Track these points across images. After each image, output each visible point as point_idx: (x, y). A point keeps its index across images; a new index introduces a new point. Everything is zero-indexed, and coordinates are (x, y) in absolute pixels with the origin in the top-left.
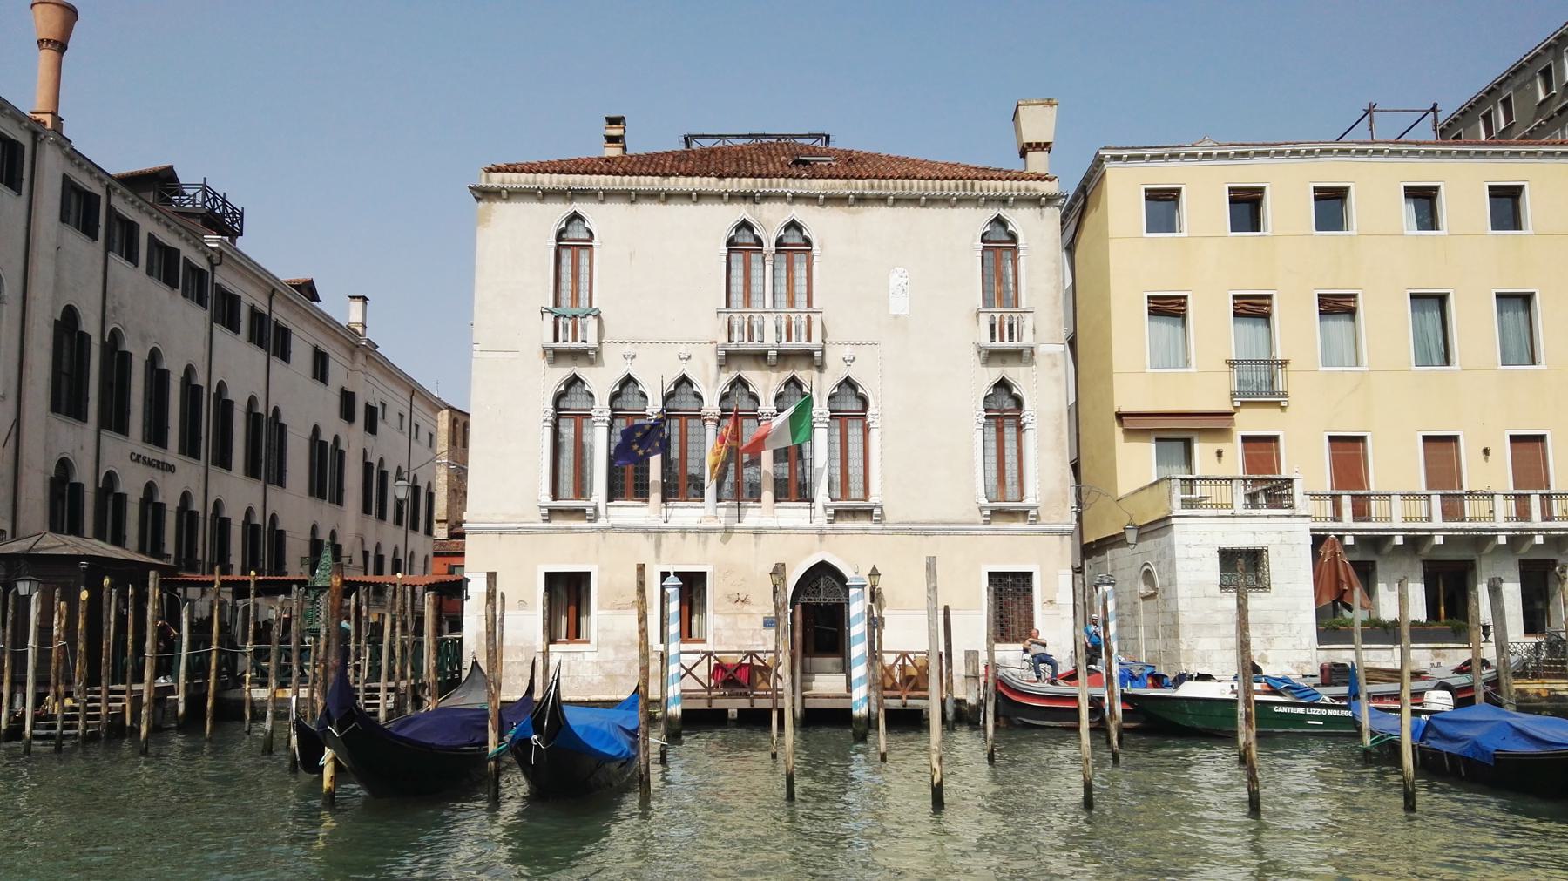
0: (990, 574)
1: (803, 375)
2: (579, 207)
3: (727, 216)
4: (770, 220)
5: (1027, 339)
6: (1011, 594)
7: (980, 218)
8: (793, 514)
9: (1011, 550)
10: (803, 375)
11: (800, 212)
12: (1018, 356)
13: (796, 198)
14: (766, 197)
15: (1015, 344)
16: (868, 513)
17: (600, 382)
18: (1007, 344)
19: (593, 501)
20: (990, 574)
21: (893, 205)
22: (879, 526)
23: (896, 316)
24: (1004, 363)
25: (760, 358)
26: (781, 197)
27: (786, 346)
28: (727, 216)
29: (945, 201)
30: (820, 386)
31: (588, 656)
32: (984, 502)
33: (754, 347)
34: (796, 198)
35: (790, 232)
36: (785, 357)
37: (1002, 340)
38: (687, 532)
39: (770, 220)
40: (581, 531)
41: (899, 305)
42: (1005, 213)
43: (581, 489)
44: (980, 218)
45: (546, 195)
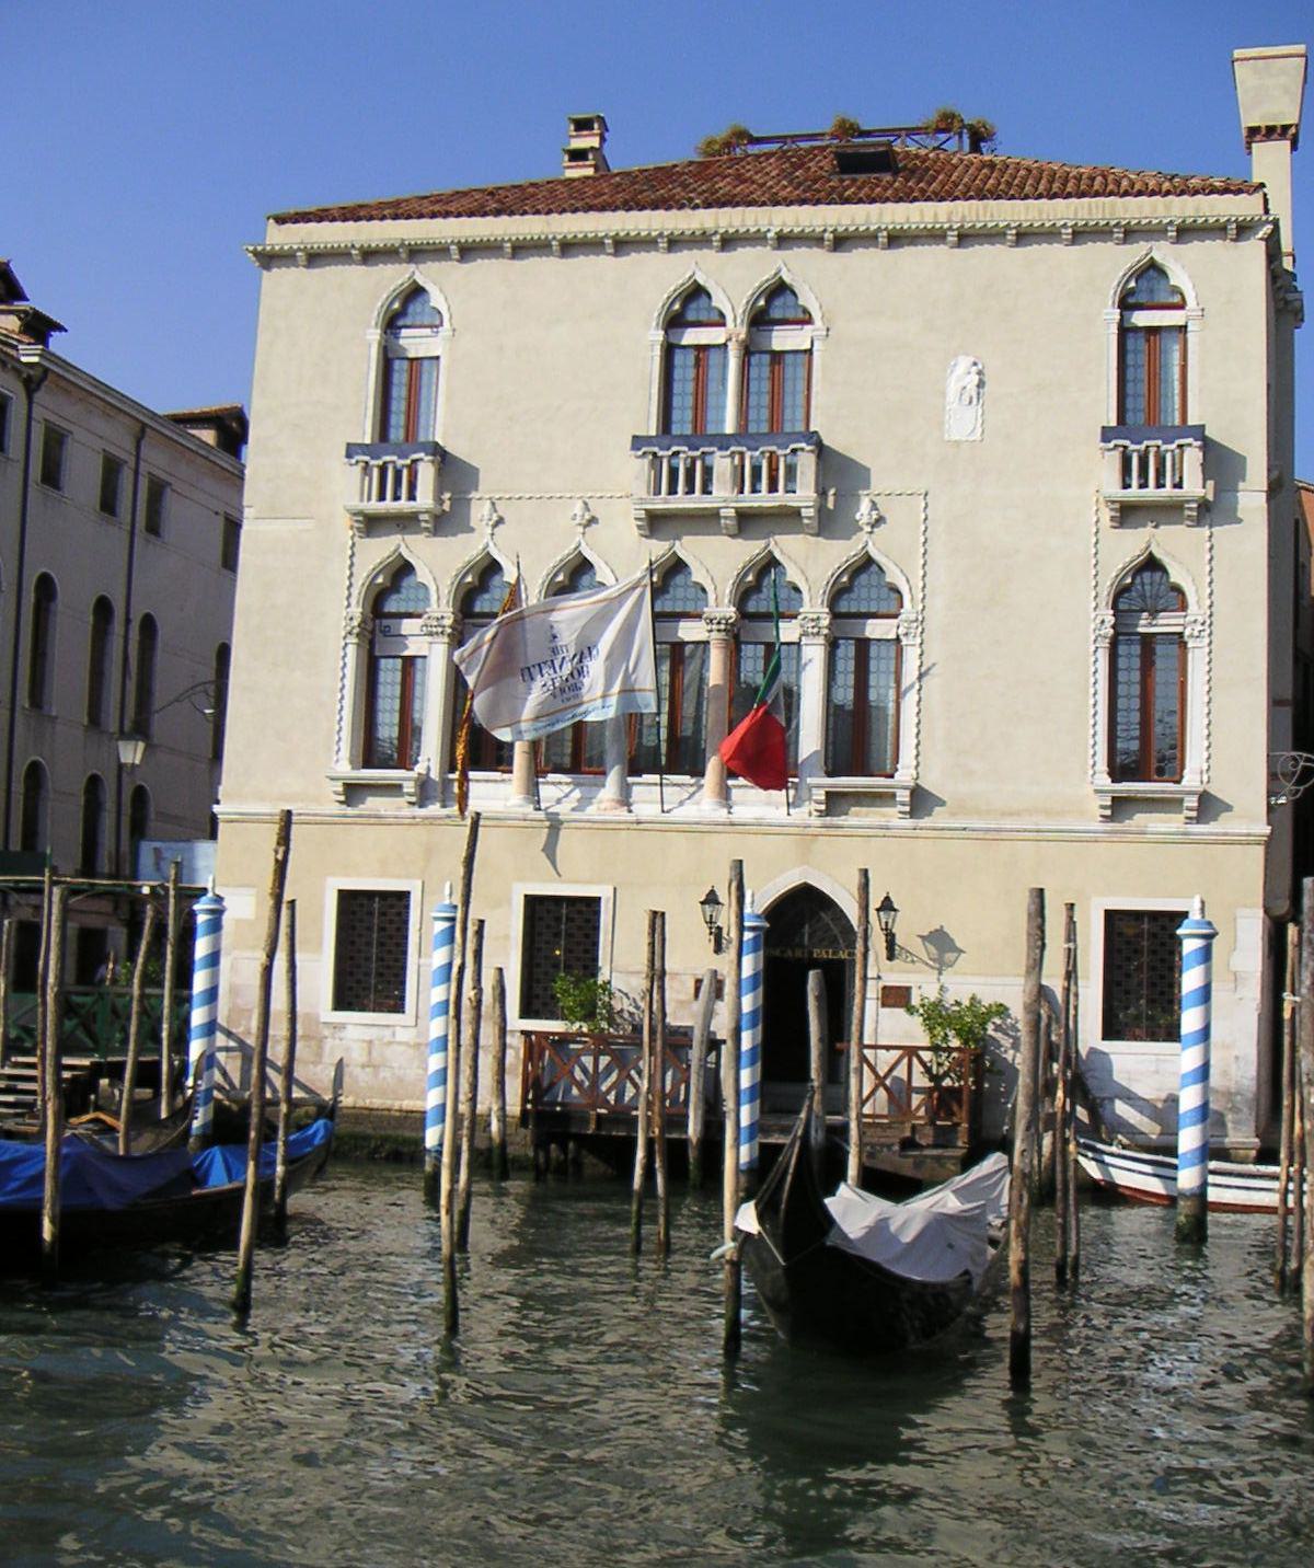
2: (425, 274)
3: (664, 274)
7: (1118, 260)
8: (755, 803)
13: (784, 240)
14: (729, 242)
17: (439, 565)
18: (1151, 493)
19: (420, 768)
21: (1125, 241)
22: (909, 822)
23: (957, 443)
28: (664, 274)
31: (404, 1035)
32: (1104, 781)
34: (784, 240)
35: (778, 302)
36: (747, 522)
39: (733, 283)
44: (1115, 262)
45: (370, 255)
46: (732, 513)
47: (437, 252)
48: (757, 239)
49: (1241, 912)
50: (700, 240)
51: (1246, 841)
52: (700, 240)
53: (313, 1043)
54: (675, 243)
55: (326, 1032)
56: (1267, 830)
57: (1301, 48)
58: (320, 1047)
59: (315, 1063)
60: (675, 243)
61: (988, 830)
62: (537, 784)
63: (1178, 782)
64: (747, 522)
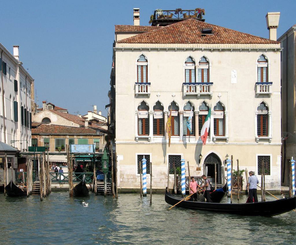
0: (258, 156)
1: (207, 100)
4: (197, 56)
5: (270, 92)
6: (264, 163)
9: (264, 150)
10: (207, 100)
11: (207, 54)
12: (268, 96)
13: (205, 50)
15: (267, 92)
16: (225, 140)
18: (265, 92)
20: (258, 156)
23: (233, 84)
24: (263, 97)
25: (196, 96)
26: (201, 49)
27: (203, 93)
29: (247, 50)
30: (212, 103)
33: (194, 93)
34: (205, 50)
36: (202, 96)
37: (263, 91)
38: (177, 145)
40: (147, 144)
41: (234, 81)
42: (265, 53)
43: (147, 133)
46: (200, 95)
47: (147, 50)
48: (201, 49)
49: (278, 156)
50: (192, 50)
51: (279, 145)
52: (192, 50)
53: (135, 179)
54: (187, 50)
55: (137, 177)
56: (282, 144)
57: (279, 13)
58: (136, 180)
59: (135, 182)
60: (187, 50)
61: (240, 144)
62: (170, 137)
63: (267, 136)
64: (202, 96)
